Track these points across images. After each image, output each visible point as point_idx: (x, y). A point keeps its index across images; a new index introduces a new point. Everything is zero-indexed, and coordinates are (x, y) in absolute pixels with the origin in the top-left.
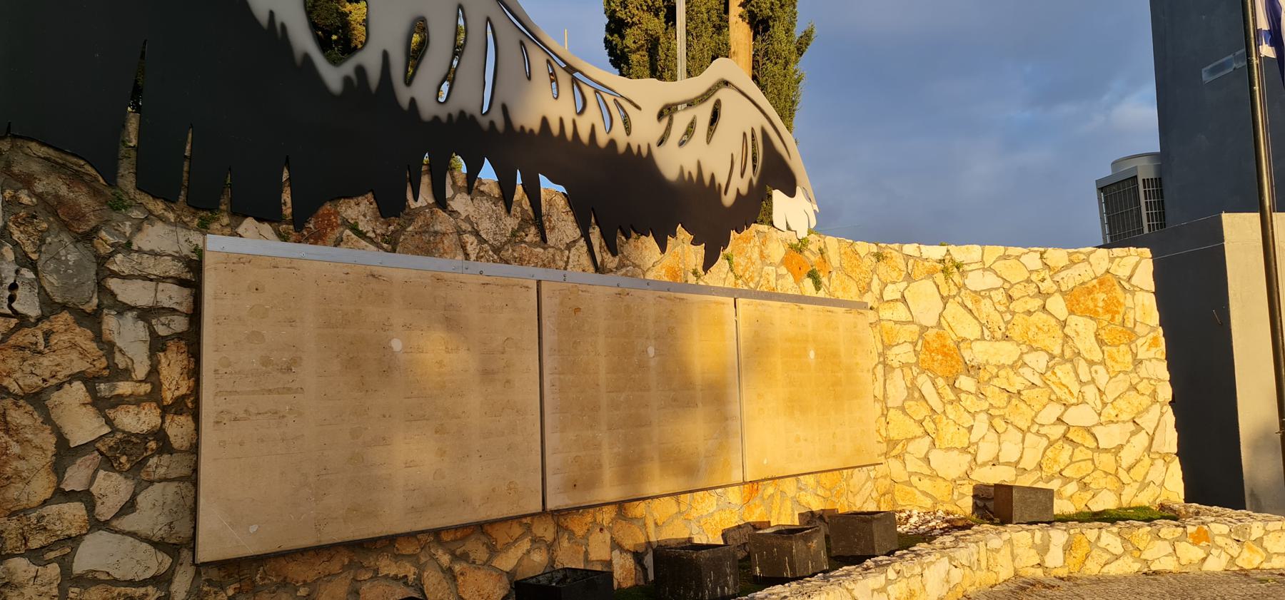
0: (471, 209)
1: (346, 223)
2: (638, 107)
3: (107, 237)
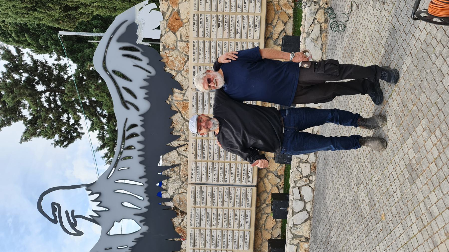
0: (172, 189)
1: (180, 224)
2: (127, 119)
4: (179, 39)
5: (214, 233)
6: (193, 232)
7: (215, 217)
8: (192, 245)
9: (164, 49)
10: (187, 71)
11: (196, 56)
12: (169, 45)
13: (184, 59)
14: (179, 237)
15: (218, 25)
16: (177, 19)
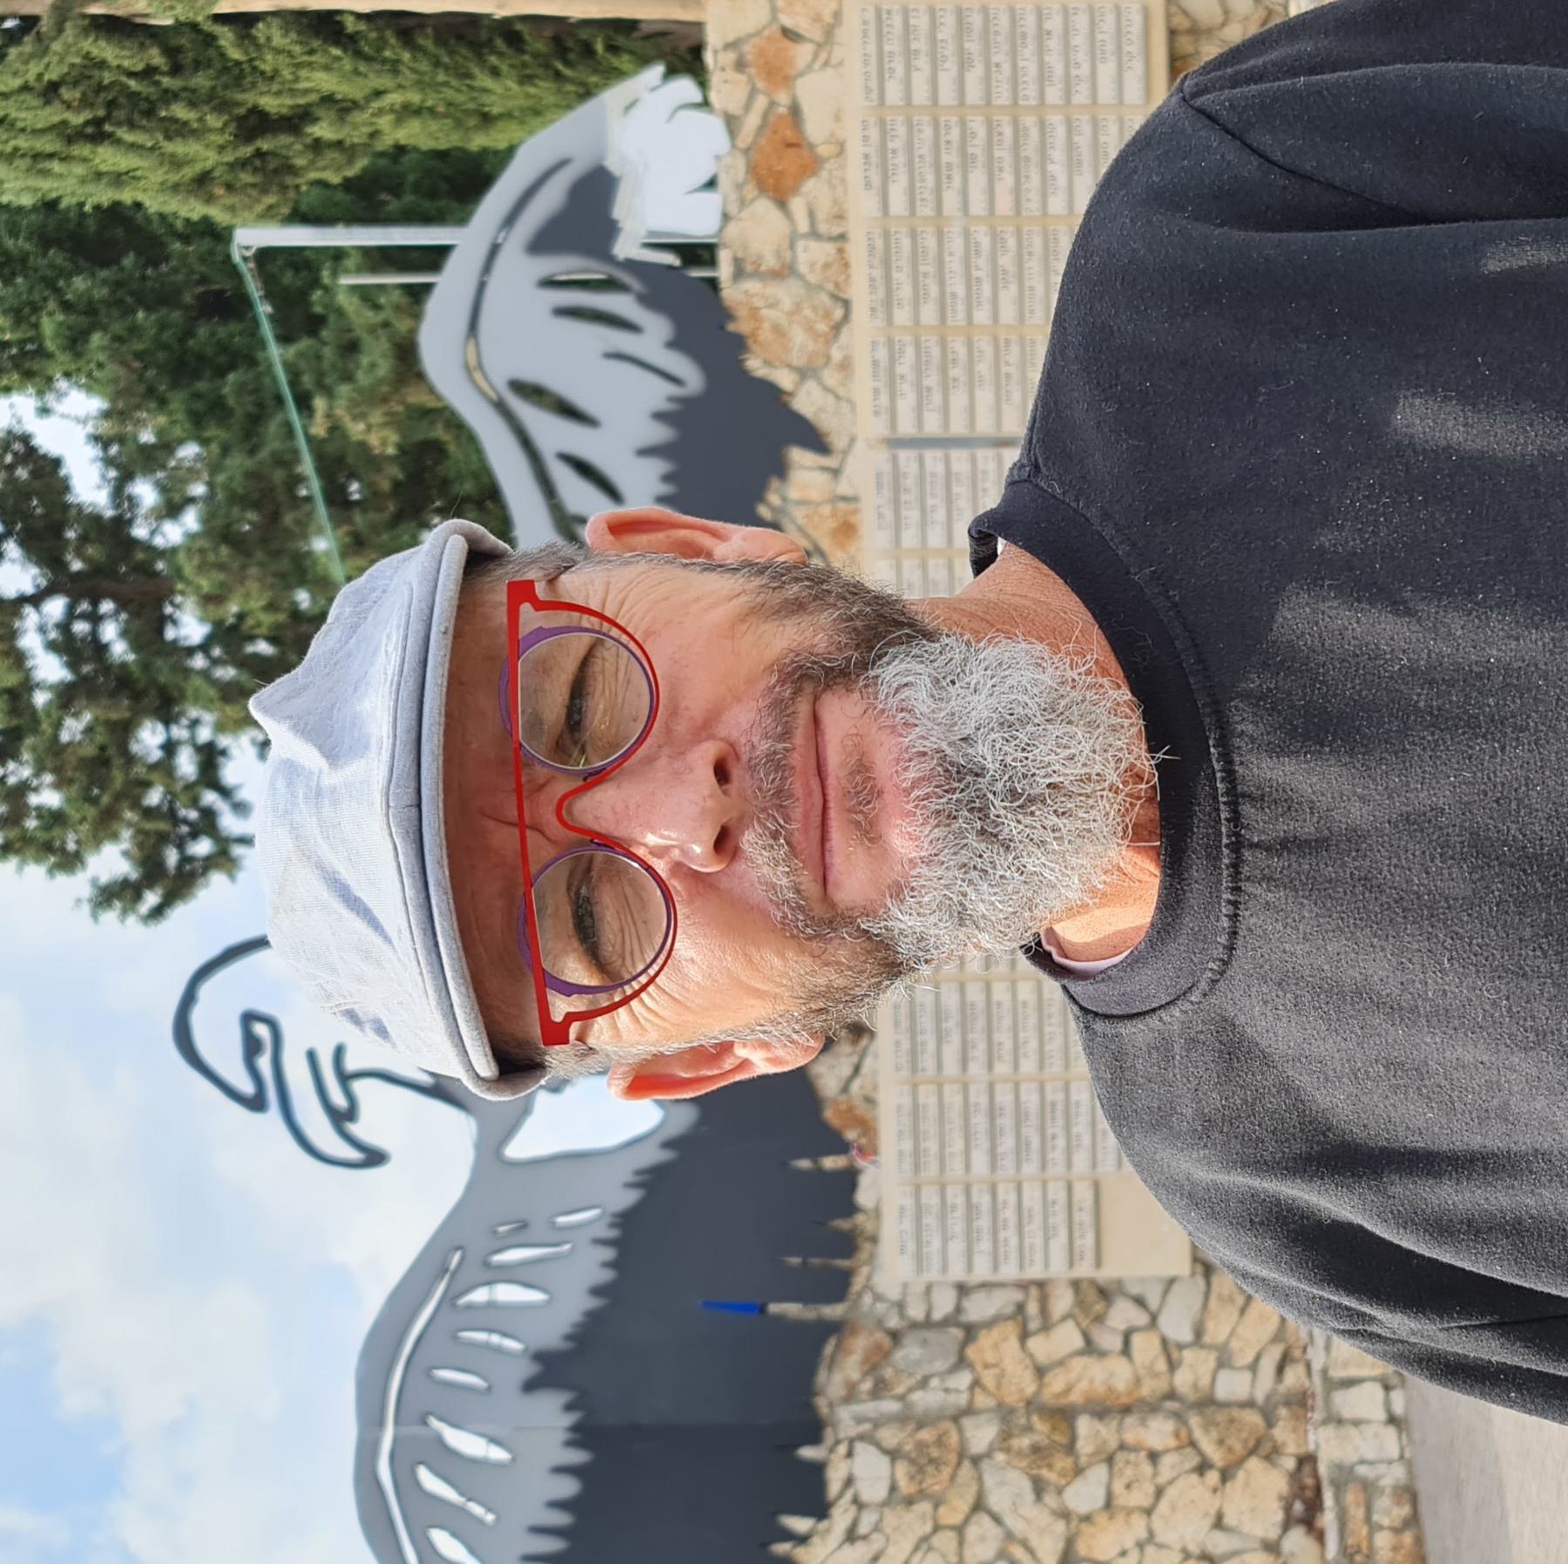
1: (845, 1089)
3: (893, 1322)
4: (803, 226)
5: (1004, 1097)
6: (907, 1101)
7: (1007, 1022)
8: (908, 1164)
9: (739, 273)
10: (845, 366)
11: (881, 292)
12: (760, 257)
13: (827, 315)
14: (842, 1147)
15: (966, 160)
16: (790, 145)
